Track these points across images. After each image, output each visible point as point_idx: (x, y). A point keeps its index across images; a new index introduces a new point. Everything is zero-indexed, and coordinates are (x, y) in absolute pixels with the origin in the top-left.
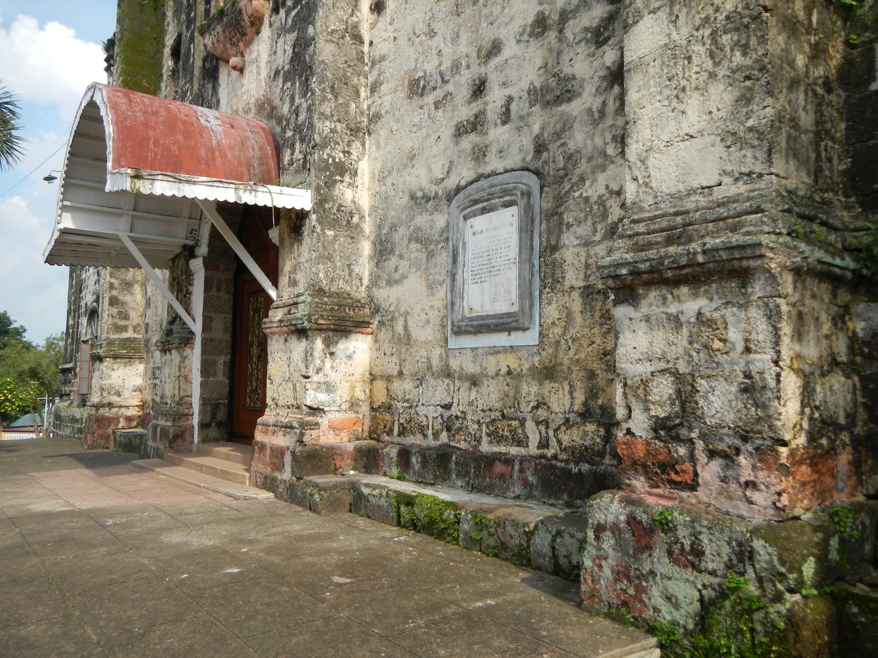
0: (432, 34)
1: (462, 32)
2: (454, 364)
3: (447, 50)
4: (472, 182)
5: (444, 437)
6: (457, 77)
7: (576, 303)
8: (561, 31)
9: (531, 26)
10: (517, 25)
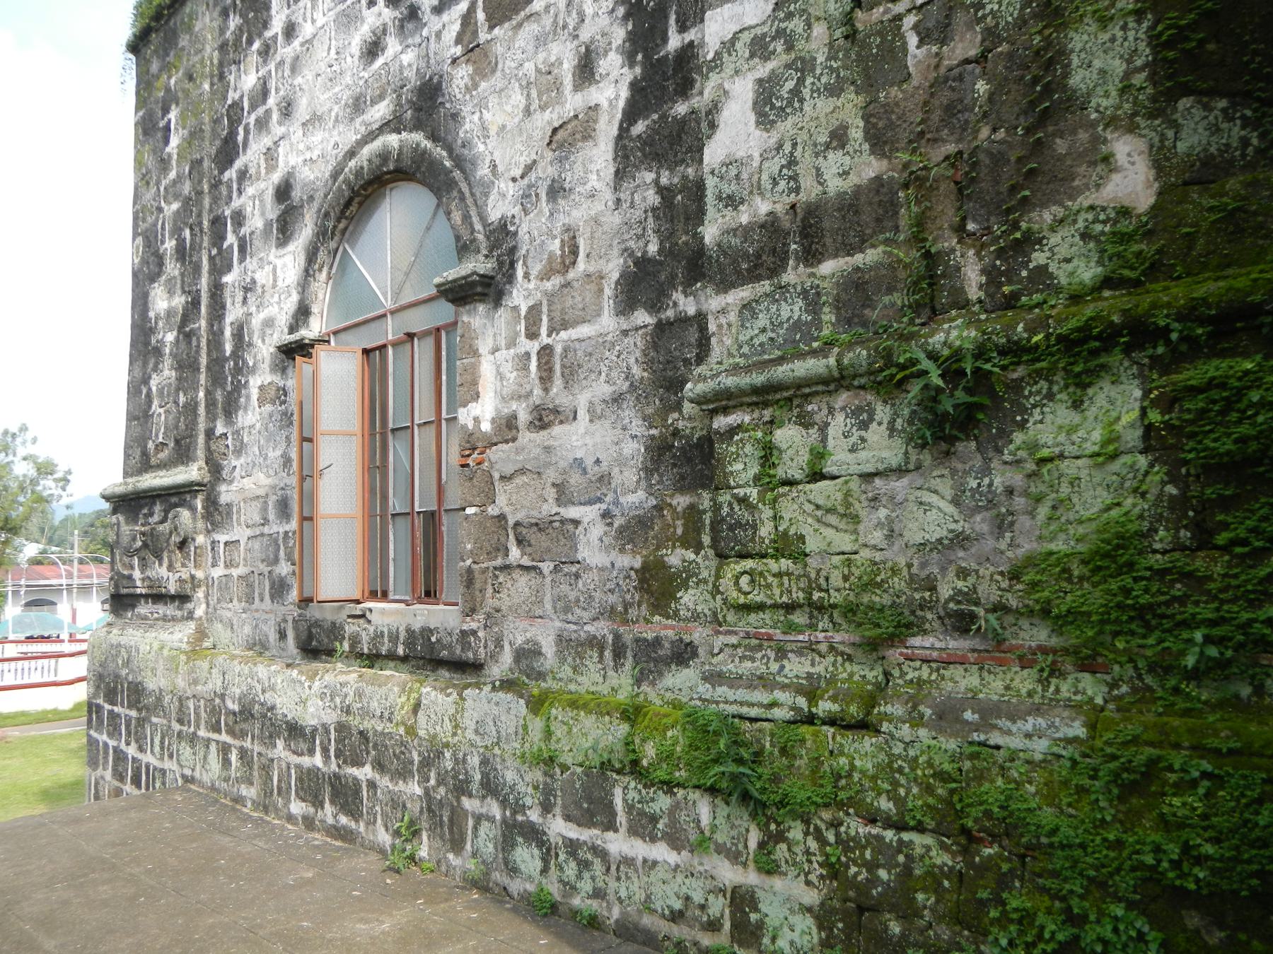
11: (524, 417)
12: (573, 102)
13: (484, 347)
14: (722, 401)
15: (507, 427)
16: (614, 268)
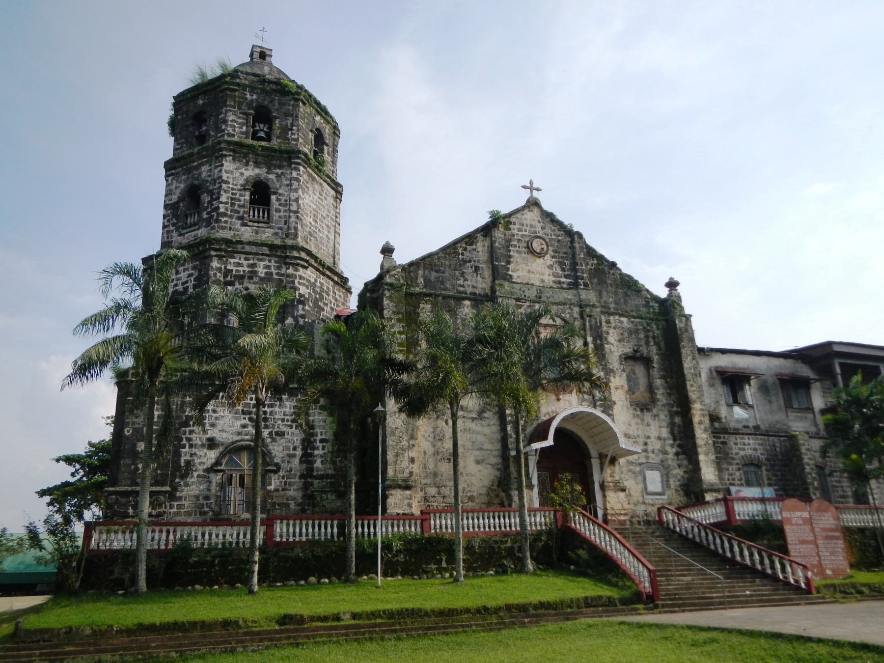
0: (630, 425)
2: (646, 501)
3: (636, 431)
5: (645, 518)
7: (674, 491)
11: (280, 489)
12: (292, 452)
13: (273, 479)
14: (316, 491)
15: (277, 490)
16: (299, 474)
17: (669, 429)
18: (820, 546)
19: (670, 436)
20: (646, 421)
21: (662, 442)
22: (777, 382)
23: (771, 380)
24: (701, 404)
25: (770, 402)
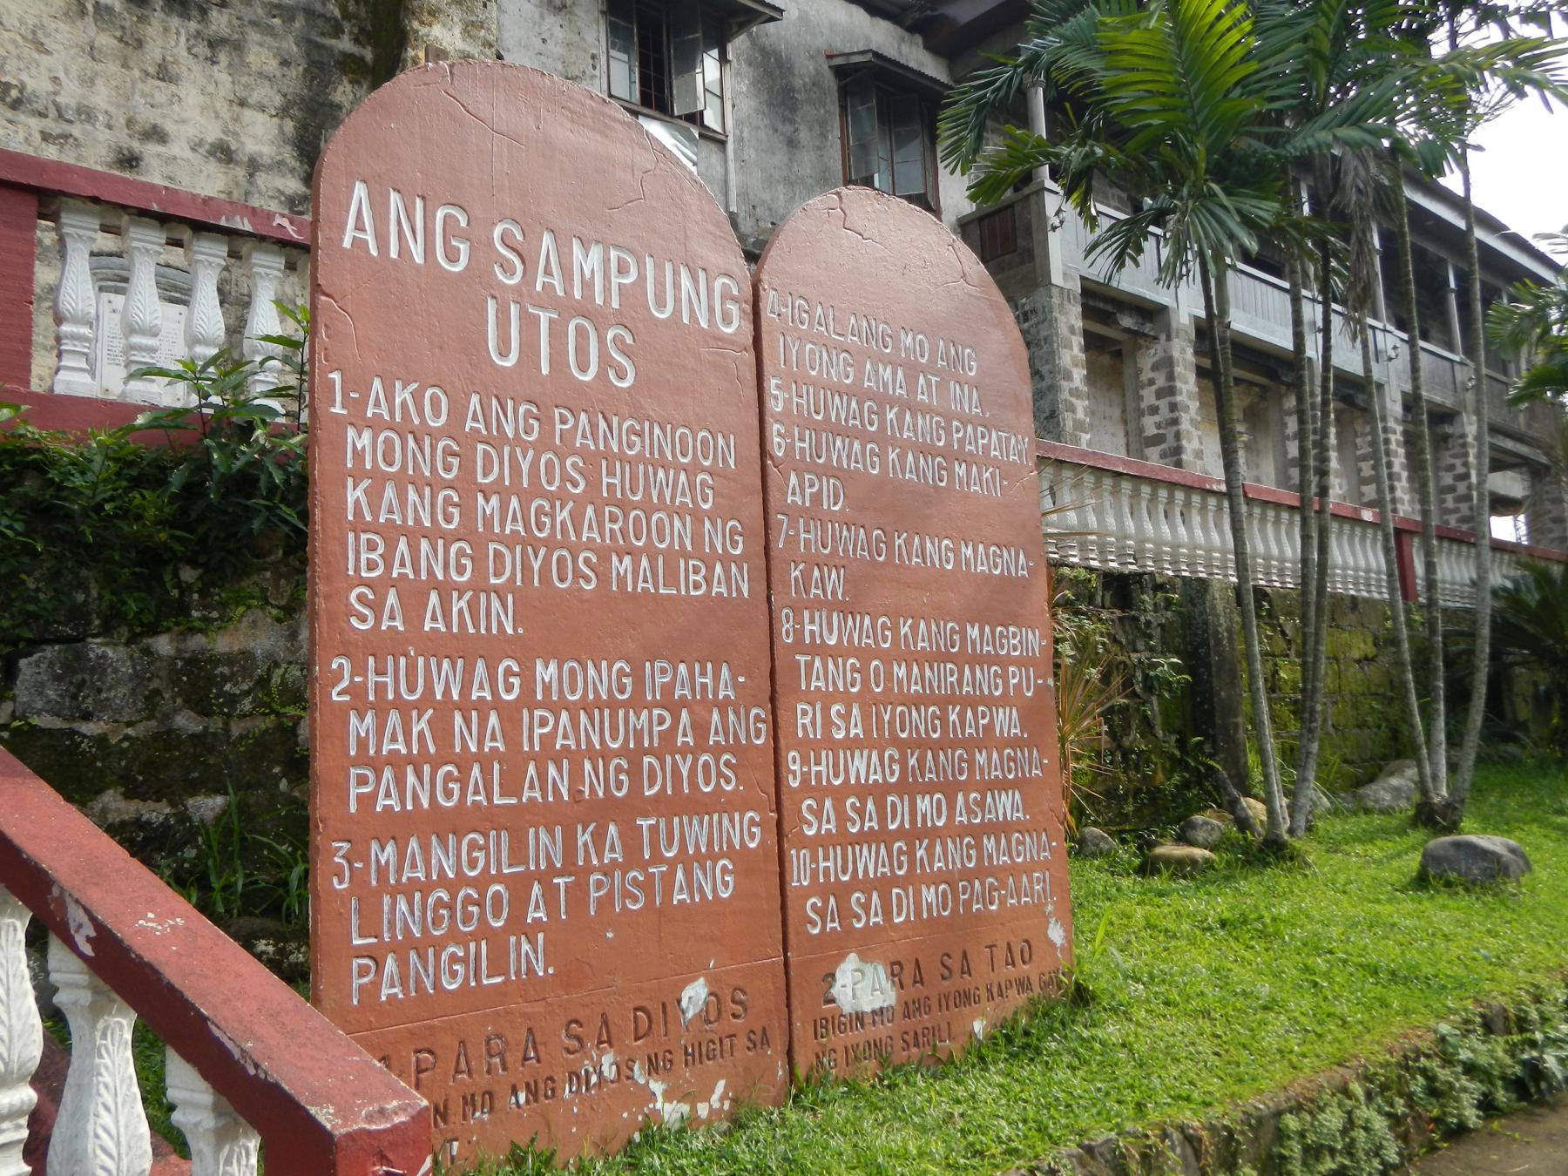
0: (41, 47)
1: (99, 82)
4: (111, 255)
6: (88, 127)
8: (251, 175)
9: (212, 145)
10: (190, 131)
17: (289, 125)
18: (819, 676)
19: (288, 155)
20: (154, 52)
21: (240, 173)
22: (830, 82)
23: (807, 68)
24: (466, 32)
25: (792, 143)
